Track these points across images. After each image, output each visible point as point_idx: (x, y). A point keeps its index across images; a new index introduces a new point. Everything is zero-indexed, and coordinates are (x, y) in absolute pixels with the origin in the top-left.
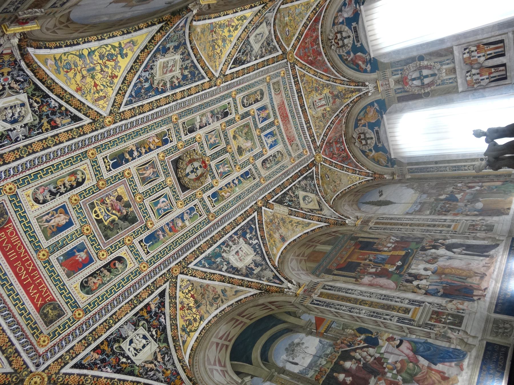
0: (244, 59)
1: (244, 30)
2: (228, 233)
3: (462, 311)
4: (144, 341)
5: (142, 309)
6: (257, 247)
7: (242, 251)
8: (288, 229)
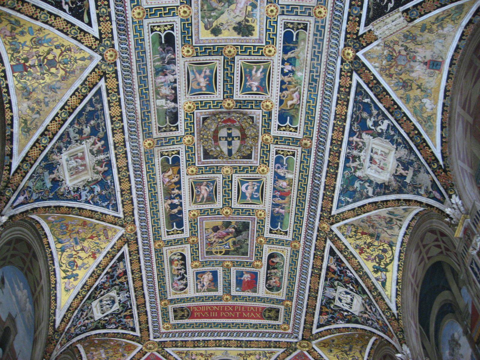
1: (19, 11)
2: (342, 141)
4: (349, 296)
5: (327, 274)
6: (392, 133)
7: (376, 153)
8: (429, 42)
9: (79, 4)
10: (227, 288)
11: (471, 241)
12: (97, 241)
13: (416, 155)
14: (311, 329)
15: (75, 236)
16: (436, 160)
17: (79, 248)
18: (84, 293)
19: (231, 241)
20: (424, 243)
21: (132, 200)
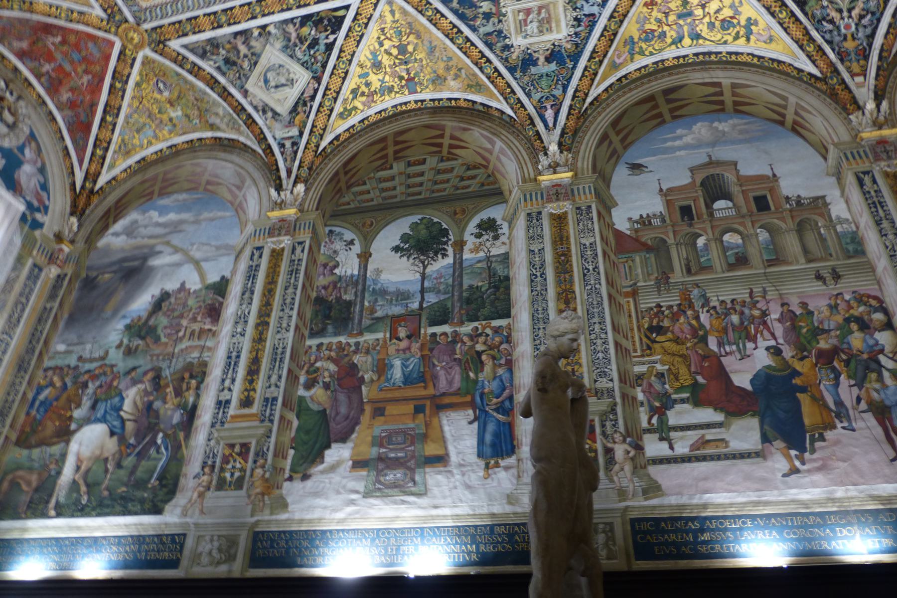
0: (305, 31)
1: (338, 93)
9: (326, 22)
15: (672, 18)
17: (699, 12)
18: (783, 15)
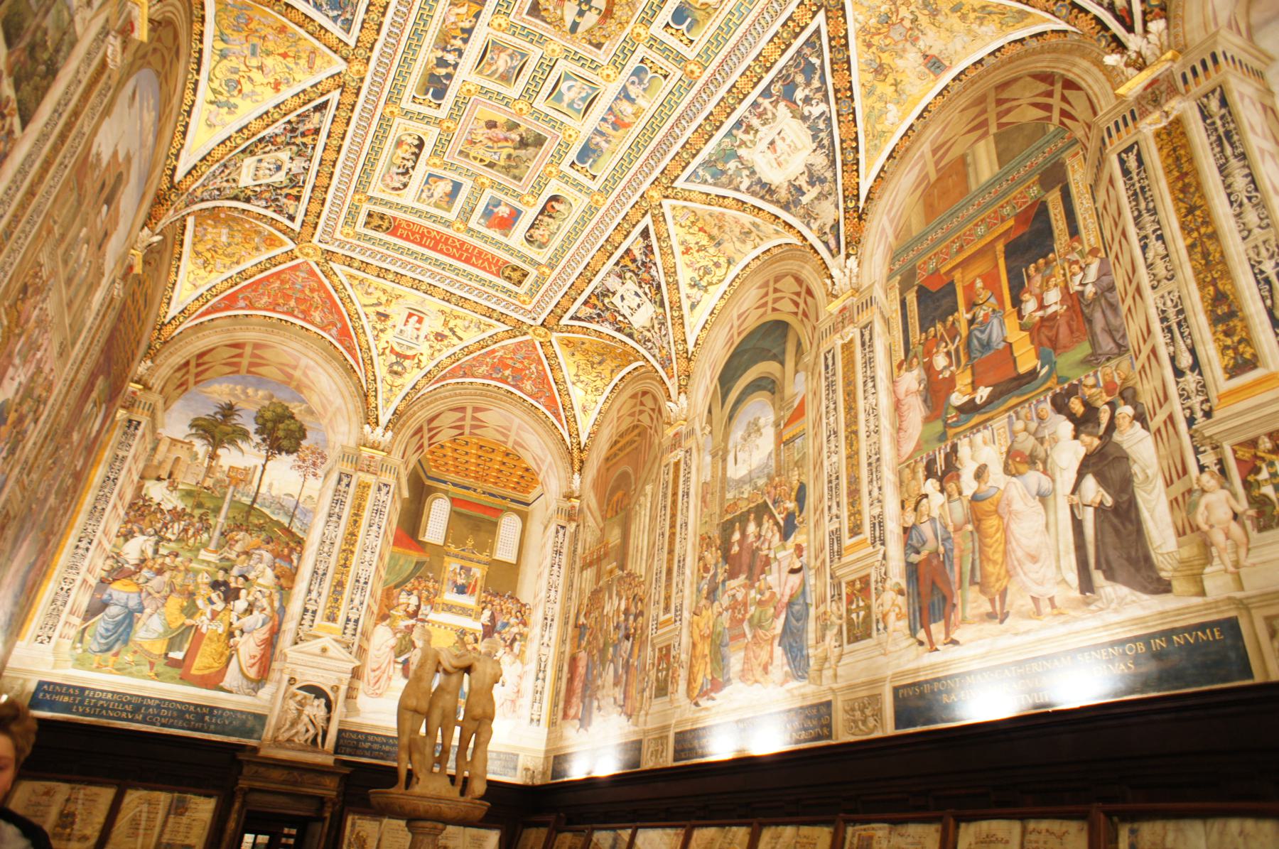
2: (745, 96)
3: (881, 626)
4: (637, 299)
5: (622, 257)
6: (822, 126)
7: (783, 139)
10: (466, 214)
11: (843, 327)
12: (292, 65)
13: (835, 175)
14: (561, 317)
15: (255, 40)
16: (857, 197)
17: (254, 62)
19: (505, 152)
20: (778, 286)
21: (380, 24)
